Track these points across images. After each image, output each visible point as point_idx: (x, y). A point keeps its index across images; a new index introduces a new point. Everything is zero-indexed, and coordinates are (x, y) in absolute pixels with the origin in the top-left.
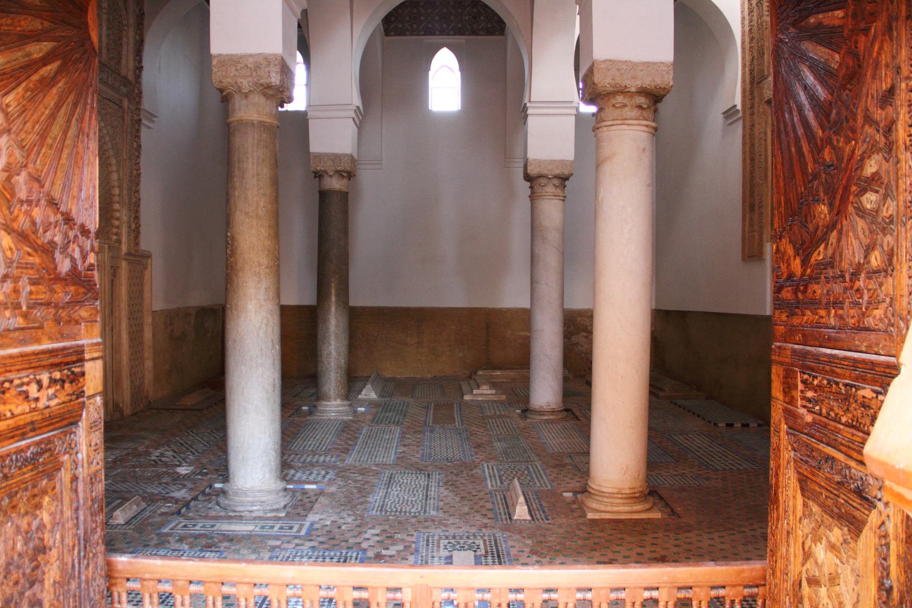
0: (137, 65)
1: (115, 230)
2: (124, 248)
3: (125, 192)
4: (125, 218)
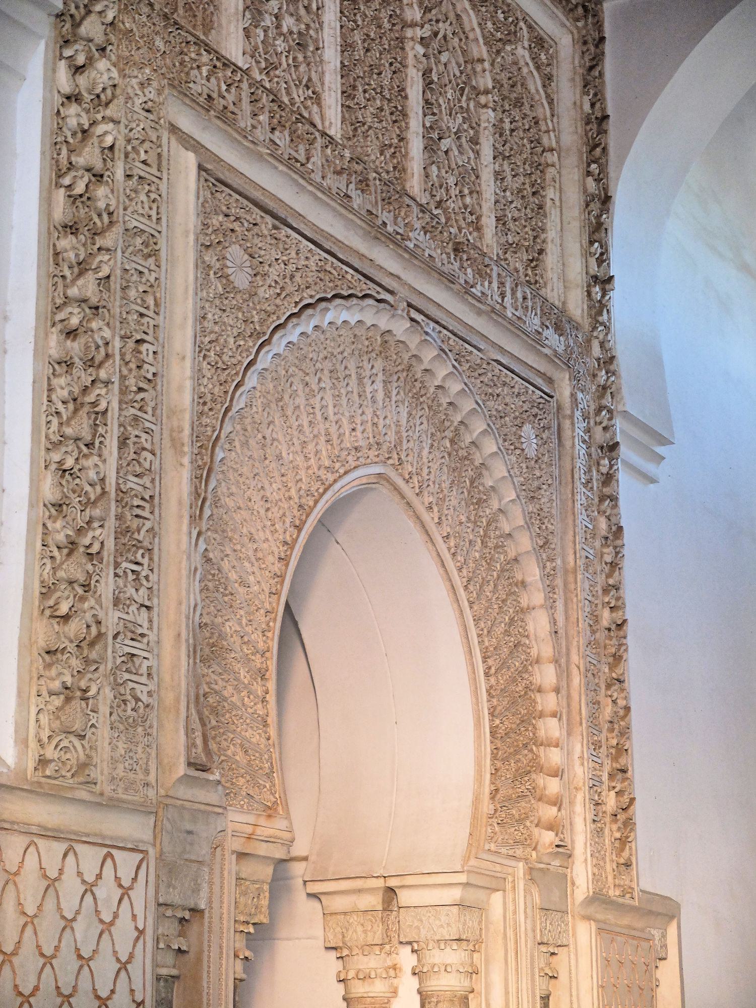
0: (594, 268)
1: (549, 812)
2: (582, 877)
3: (577, 680)
4: (580, 773)
